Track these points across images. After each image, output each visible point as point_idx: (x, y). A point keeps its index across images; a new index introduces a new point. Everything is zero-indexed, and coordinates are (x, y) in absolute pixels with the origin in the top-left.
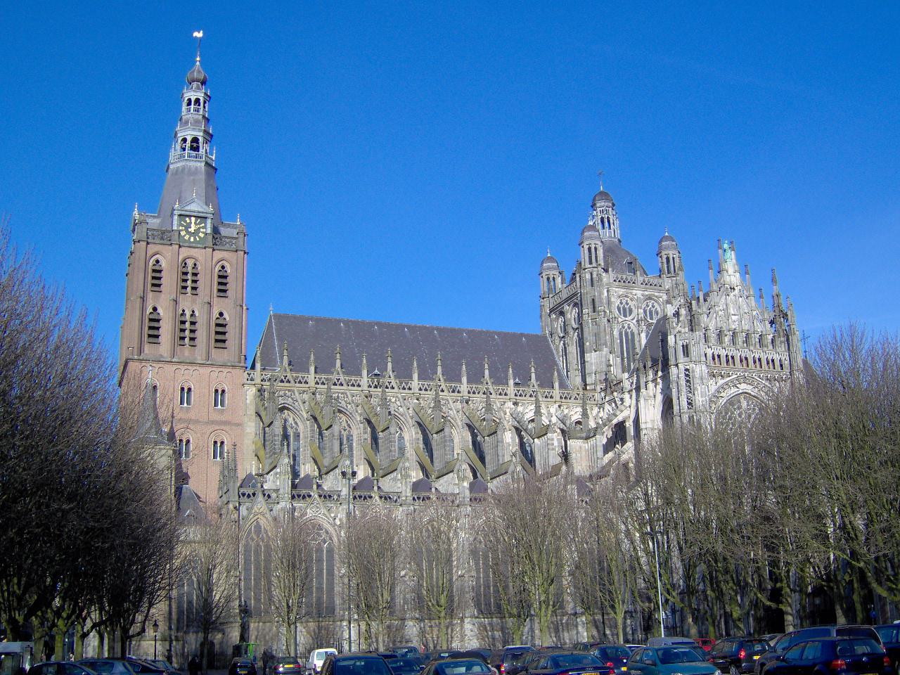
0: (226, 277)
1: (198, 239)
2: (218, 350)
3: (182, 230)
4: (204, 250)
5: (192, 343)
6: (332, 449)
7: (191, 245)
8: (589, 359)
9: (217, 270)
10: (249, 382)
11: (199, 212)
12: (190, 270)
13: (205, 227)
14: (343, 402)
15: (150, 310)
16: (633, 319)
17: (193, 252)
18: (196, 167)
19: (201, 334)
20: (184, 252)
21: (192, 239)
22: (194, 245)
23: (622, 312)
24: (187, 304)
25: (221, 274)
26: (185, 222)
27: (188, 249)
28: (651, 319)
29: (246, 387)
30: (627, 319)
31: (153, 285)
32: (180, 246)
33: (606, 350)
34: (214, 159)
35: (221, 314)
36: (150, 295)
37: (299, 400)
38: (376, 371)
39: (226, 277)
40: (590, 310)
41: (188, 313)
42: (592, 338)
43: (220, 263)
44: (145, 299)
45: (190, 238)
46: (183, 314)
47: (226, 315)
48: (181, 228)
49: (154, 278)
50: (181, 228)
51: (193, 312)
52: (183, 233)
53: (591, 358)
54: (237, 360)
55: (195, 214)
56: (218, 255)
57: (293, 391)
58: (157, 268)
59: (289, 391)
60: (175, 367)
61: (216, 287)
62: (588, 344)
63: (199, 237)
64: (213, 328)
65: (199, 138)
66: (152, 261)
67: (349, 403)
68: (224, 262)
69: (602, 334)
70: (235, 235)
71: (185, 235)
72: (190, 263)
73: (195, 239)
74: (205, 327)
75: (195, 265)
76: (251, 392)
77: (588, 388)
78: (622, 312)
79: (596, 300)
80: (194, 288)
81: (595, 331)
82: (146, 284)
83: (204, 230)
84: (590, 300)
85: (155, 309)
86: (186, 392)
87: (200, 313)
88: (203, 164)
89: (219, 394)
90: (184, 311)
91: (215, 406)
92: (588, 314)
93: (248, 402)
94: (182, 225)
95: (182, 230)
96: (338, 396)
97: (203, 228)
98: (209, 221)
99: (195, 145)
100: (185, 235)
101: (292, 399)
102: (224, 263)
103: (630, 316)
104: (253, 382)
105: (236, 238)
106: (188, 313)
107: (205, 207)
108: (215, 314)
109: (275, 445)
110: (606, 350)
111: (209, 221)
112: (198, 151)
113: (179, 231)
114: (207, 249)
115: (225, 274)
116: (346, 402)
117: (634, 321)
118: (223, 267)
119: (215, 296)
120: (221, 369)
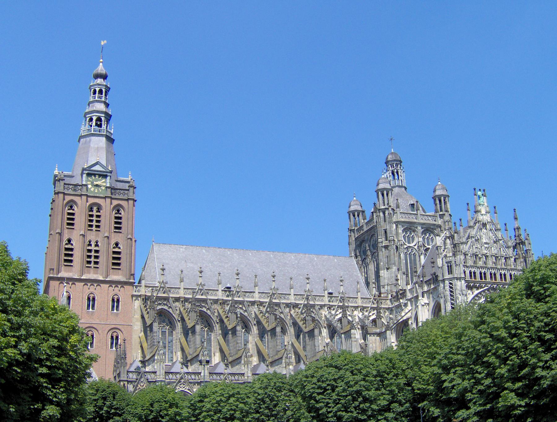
1: (101, 191)
2: (115, 270)
3: (89, 184)
6: (195, 342)
8: (383, 275)
15: (65, 241)
16: (415, 246)
21: (96, 191)
22: (98, 195)
23: (407, 240)
24: (92, 236)
25: (117, 215)
28: (428, 244)
30: (410, 245)
33: (394, 268)
34: (112, 133)
35: (117, 244)
36: (66, 231)
39: (120, 218)
40: (383, 239)
41: (93, 244)
42: (385, 260)
44: (62, 234)
45: (94, 190)
46: (90, 245)
48: (88, 183)
49: (68, 219)
50: (88, 183)
52: (90, 186)
53: (384, 274)
61: (113, 225)
62: (382, 263)
63: (102, 189)
65: (102, 118)
69: (392, 257)
70: (127, 188)
73: (98, 190)
74: (105, 254)
77: (382, 295)
78: (407, 240)
79: (388, 232)
80: (98, 226)
81: (387, 254)
82: (63, 224)
83: (105, 184)
84: (383, 232)
85: (69, 241)
86: (91, 301)
87: (101, 244)
89: (116, 302)
91: (112, 311)
92: (382, 242)
93: (136, 307)
94: (89, 181)
99: (99, 123)
103: (412, 243)
105: (128, 190)
109: (154, 339)
110: (394, 268)
112: (101, 127)
115: (120, 216)
117: (416, 247)
119: (112, 231)
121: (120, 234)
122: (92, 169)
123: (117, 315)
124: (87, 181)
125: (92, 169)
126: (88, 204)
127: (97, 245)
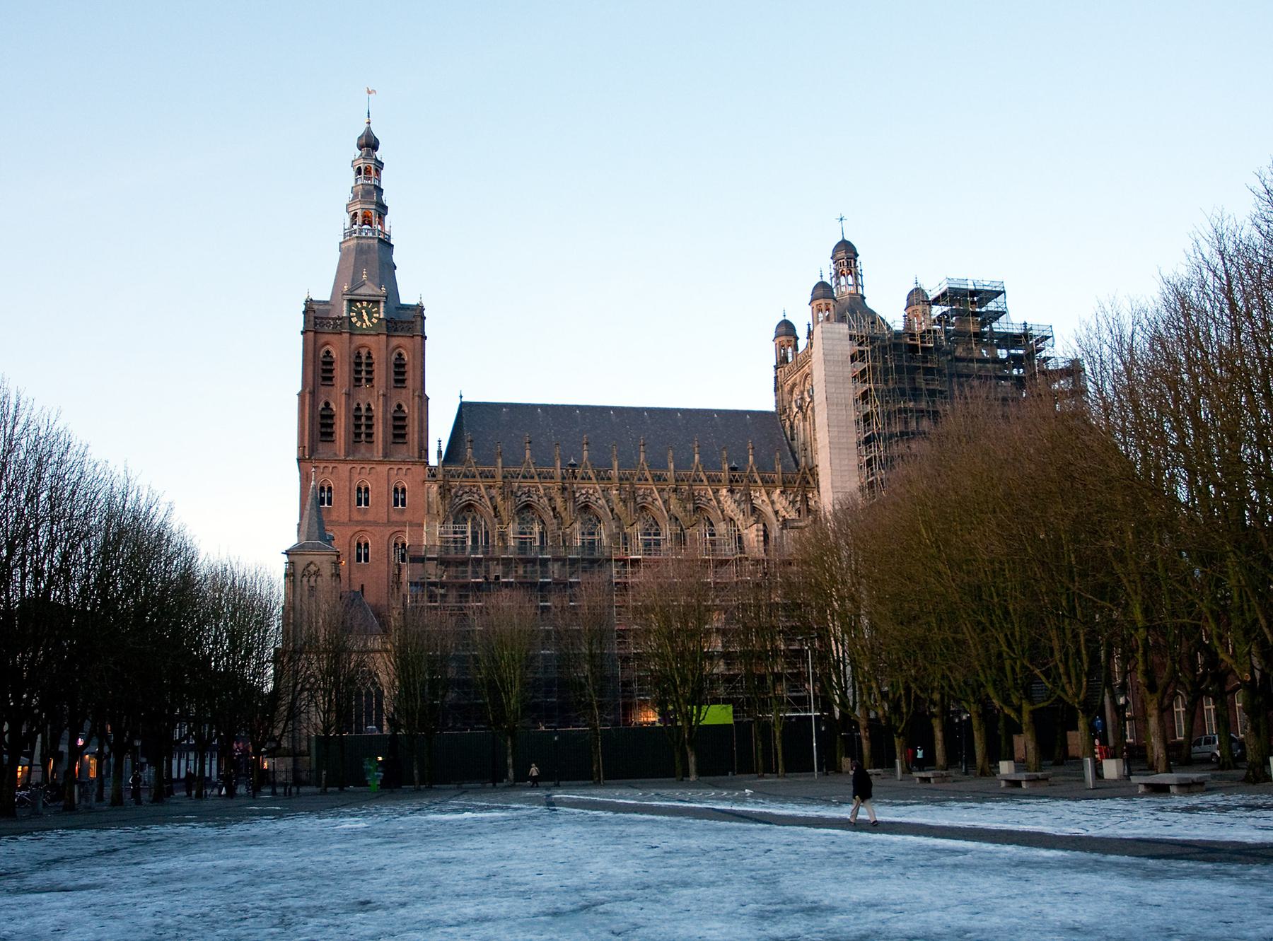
0: (403, 366)
3: (353, 317)
4: (376, 338)
5: (369, 440)
7: (363, 332)
9: (393, 358)
10: (430, 479)
11: (370, 296)
12: (364, 359)
13: (378, 312)
14: (535, 497)
15: (322, 405)
17: (365, 340)
18: (369, 246)
19: (379, 431)
20: (359, 340)
22: (366, 332)
26: (357, 307)
27: (360, 337)
29: (427, 484)
31: (324, 379)
32: (351, 334)
37: (486, 497)
38: (572, 461)
41: (363, 407)
43: (397, 350)
46: (359, 409)
47: (405, 408)
48: (351, 314)
50: (351, 314)
51: (369, 405)
52: (354, 320)
54: (416, 455)
55: (366, 298)
56: (395, 342)
57: (479, 487)
58: (328, 359)
59: (474, 486)
60: (350, 466)
64: (391, 422)
66: (322, 353)
67: (542, 497)
68: (400, 349)
71: (356, 322)
72: (364, 352)
75: (369, 353)
76: (435, 488)
80: (369, 380)
87: (377, 406)
88: (376, 241)
90: (358, 404)
94: (354, 311)
95: (353, 317)
96: (529, 491)
97: (376, 312)
98: (382, 305)
100: (356, 322)
101: (479, 495)
102: (403, 351)
104: (435, 479)
106: (363, 407)
107: (379, 290)
108: (394, 407)
111: (382, 305)
113: (350, 318)
114: (381, 336)
115: (403, 362)
116: (538, 495)
118: (400, 355)
120: (400, 466)
121: (404, 391)
122: (356, 292)
123: (403, 512)
124: (350, 311)
125: (356, 292)
126: (353, 346)
127: (369, 409)
